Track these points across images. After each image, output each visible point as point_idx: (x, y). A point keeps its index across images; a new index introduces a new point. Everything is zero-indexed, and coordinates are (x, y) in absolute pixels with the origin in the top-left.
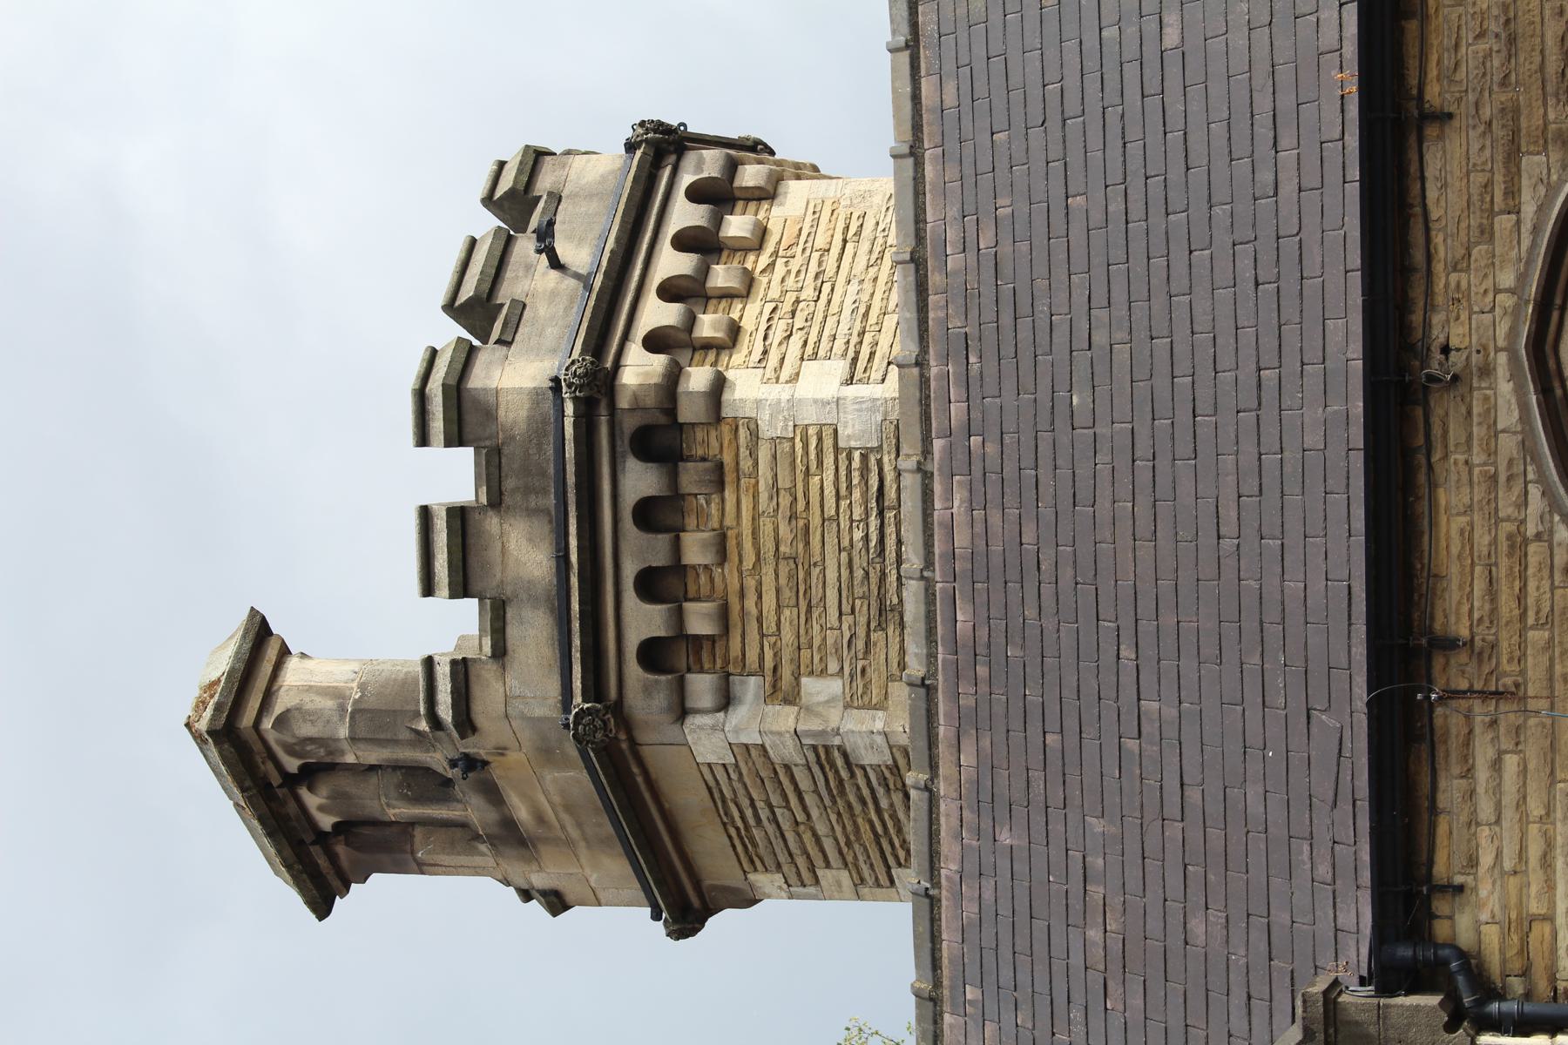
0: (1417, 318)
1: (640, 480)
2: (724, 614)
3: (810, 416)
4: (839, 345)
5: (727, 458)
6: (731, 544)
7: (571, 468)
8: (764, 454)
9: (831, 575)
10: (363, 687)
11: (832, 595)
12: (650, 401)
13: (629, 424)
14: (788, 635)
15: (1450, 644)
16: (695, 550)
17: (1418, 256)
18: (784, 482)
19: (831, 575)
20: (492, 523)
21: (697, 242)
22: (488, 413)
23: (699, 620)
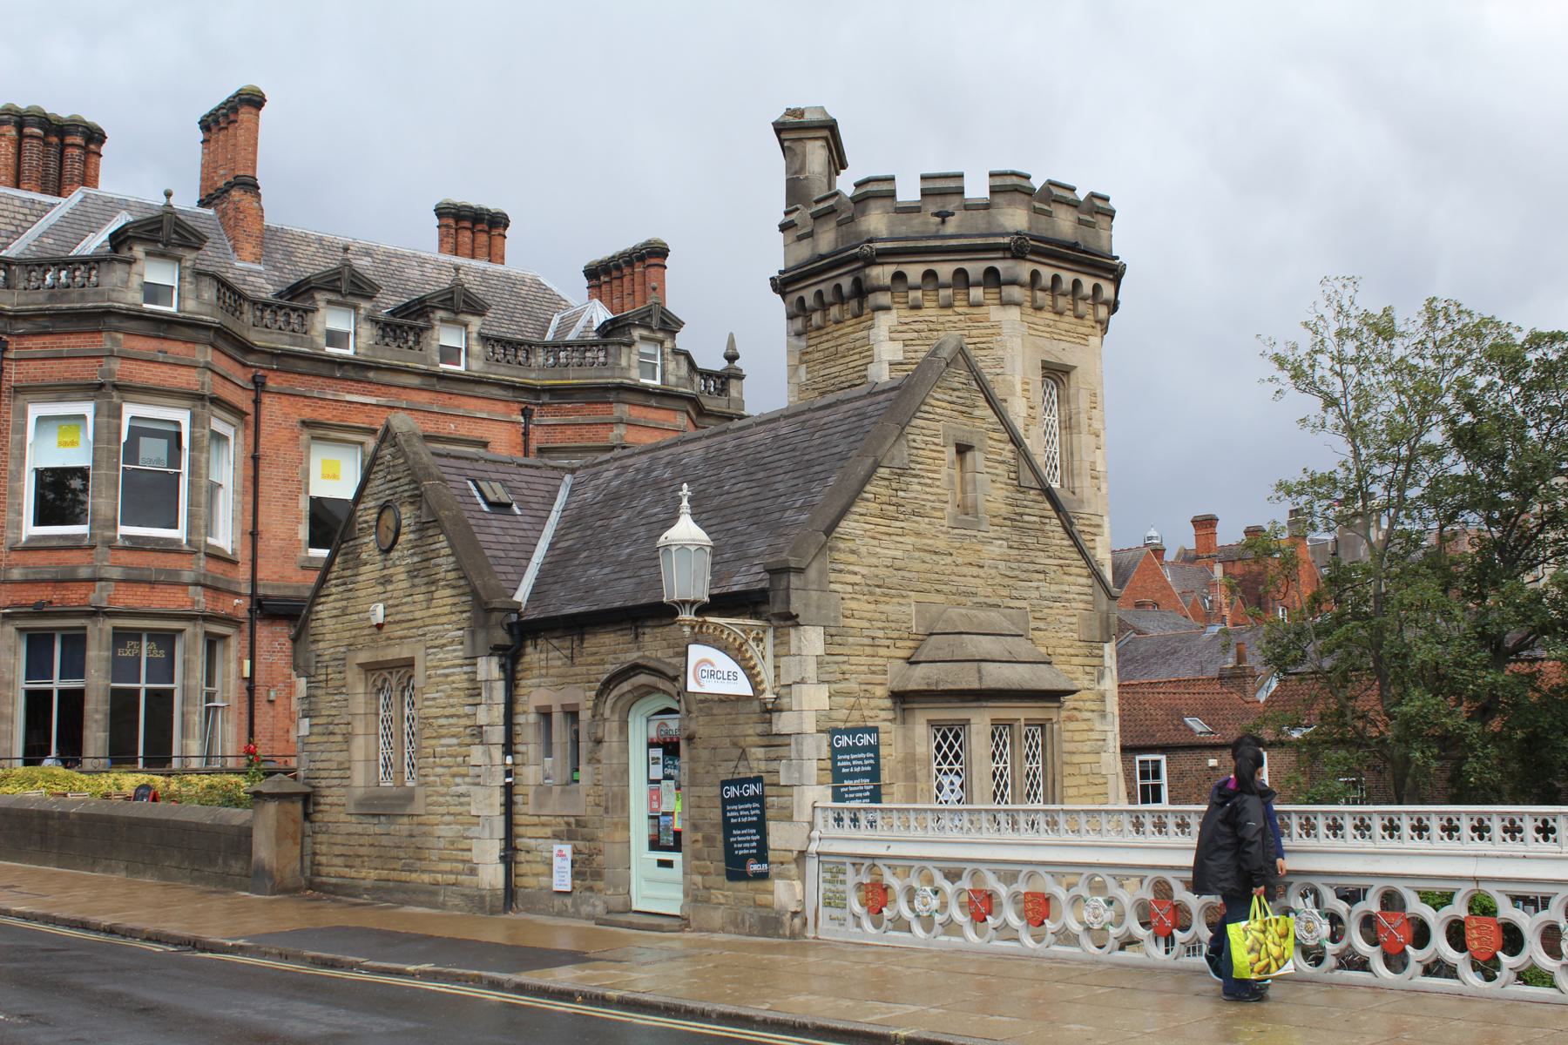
0: (650, 623)
1: (846, 283)
2: (819, 328)
3: (876, 350)
4: (913, 355)
5: (863, 318)
6: (840, 326)
7: (845, 255)
8: (864, 333)
9: (833, 370)
10: (807, 178)
11: (827, 372)
12: (868, 283)
13: (861, 275)
14: (816, 355)
15: (582, 641)
16: (834, 311)
17: (664, 622)
18: (858, 344)
19: (833, 370)
20: (833, 224)
21: (962, 279)
22: (863, 213)
23: (816, 318)
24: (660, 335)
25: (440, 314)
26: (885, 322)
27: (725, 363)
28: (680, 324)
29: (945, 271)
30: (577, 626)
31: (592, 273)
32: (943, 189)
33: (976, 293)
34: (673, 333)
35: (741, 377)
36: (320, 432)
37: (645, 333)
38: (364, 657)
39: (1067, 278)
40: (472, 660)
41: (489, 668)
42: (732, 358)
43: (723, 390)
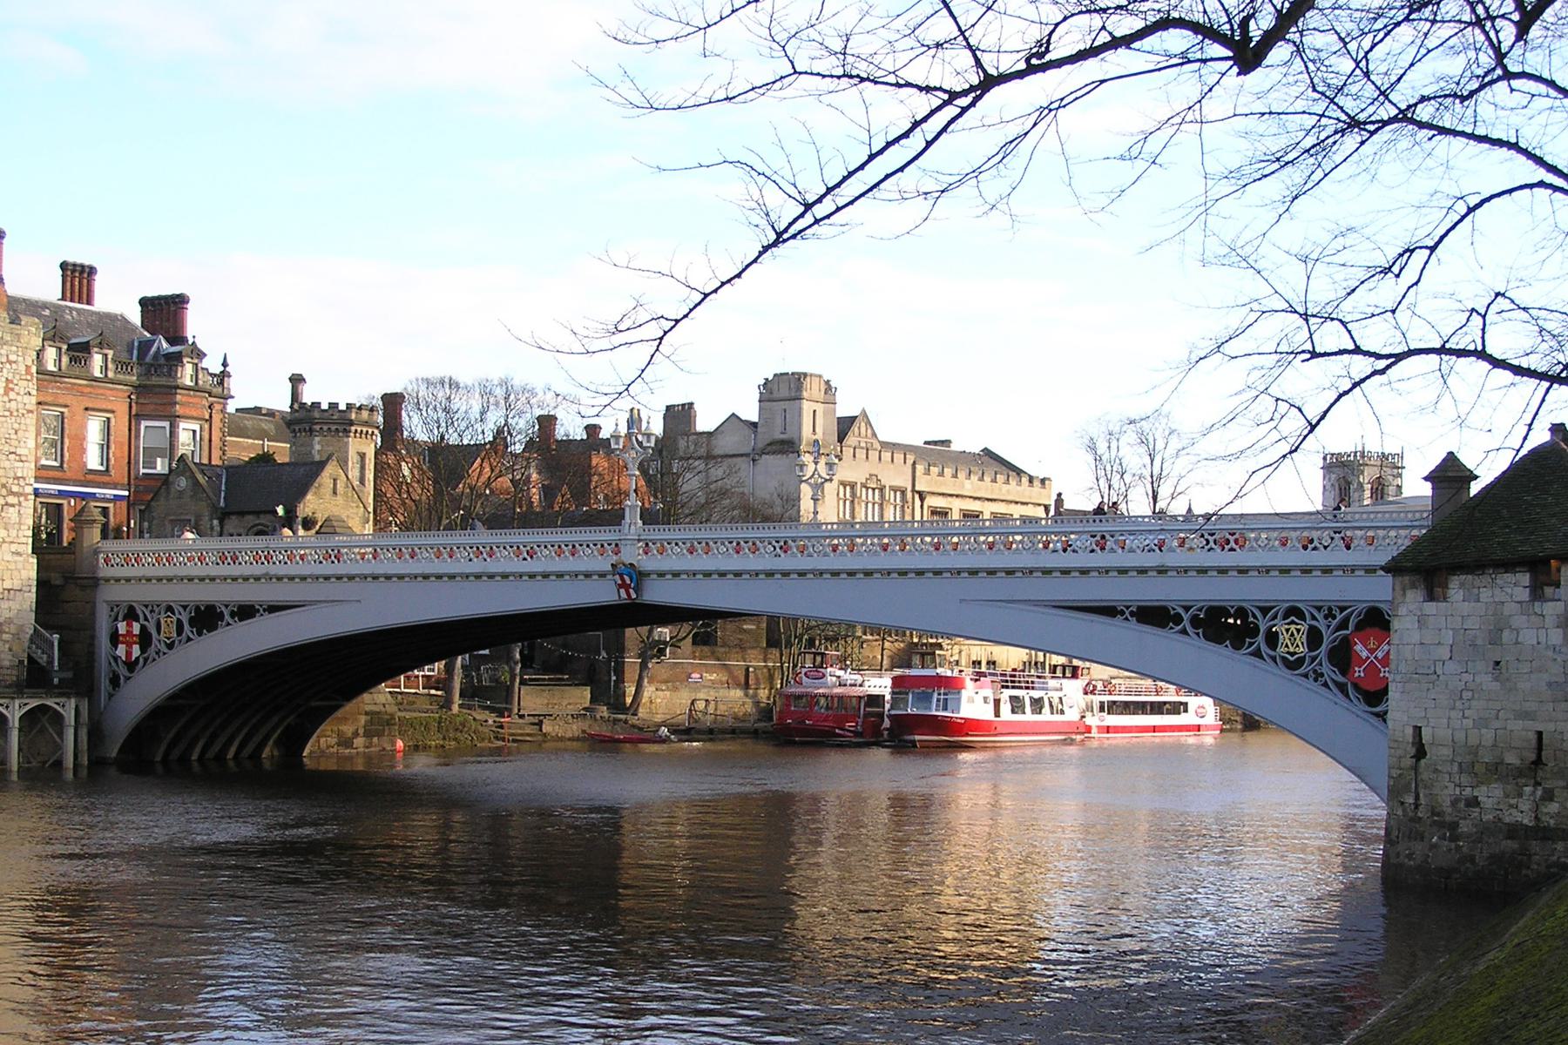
24: (196, 361)
25: (96, 349)
26: (317, 439)
27: (222, 369)
28: (205, 355)
29: (333, 428)
30: (242, 514)
31: (144, 302)
32: (333, 406)
33: (341, 434)
34: (201, 360)
35: (229, 376)
36: (46, 407)
37: (189, 360)
38: (172, 518)
39: (365, 430)
40: (211, 520)
41: (216, 522)
42: (225, 364)
43: (221, 383)
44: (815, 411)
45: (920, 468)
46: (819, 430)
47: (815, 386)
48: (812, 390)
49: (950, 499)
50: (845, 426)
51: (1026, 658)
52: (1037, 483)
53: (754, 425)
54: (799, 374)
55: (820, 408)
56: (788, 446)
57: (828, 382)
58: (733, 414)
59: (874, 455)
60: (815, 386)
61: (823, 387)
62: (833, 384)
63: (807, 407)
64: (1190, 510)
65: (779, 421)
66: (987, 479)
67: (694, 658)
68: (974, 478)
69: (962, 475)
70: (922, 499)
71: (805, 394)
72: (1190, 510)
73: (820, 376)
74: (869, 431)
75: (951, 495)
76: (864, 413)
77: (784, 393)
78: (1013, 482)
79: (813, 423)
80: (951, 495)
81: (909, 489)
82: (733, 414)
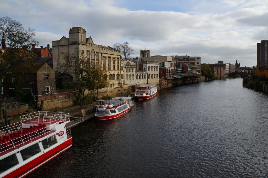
44: (81, 35)
45: (101, 48)
46: (82, 39)
47: (81, 30)
48: (81, 31)
49: (106, 54)
50: (87, 39)
51: (118, 83)
52: (119, 52)
53: (68, 39)
54: (78, 27)
55: (82, 35)
56: (76, 43)
57: (84, 30)
58: (64, 37)
59: (93, 45)
60: (81, 30)
61: (83, 30)
62: (85, 30)
63: (80, 34)
64: (137, 57)
65: (74, 37)
66: (112, 51)
67: (57, 92)
68: (110, 51)
69: (108, 50)
70: (102, 54)
71: (80, 32)
72: (137, 57)
73: (82, 28)
74: (92, 41)
75: (106, 54)
76: (90, 37)
77: (75, 32)
78: (116, 52)
79: (81, 38)
80: (106, 54)
81: (99, 52)
82: (64, 37)
